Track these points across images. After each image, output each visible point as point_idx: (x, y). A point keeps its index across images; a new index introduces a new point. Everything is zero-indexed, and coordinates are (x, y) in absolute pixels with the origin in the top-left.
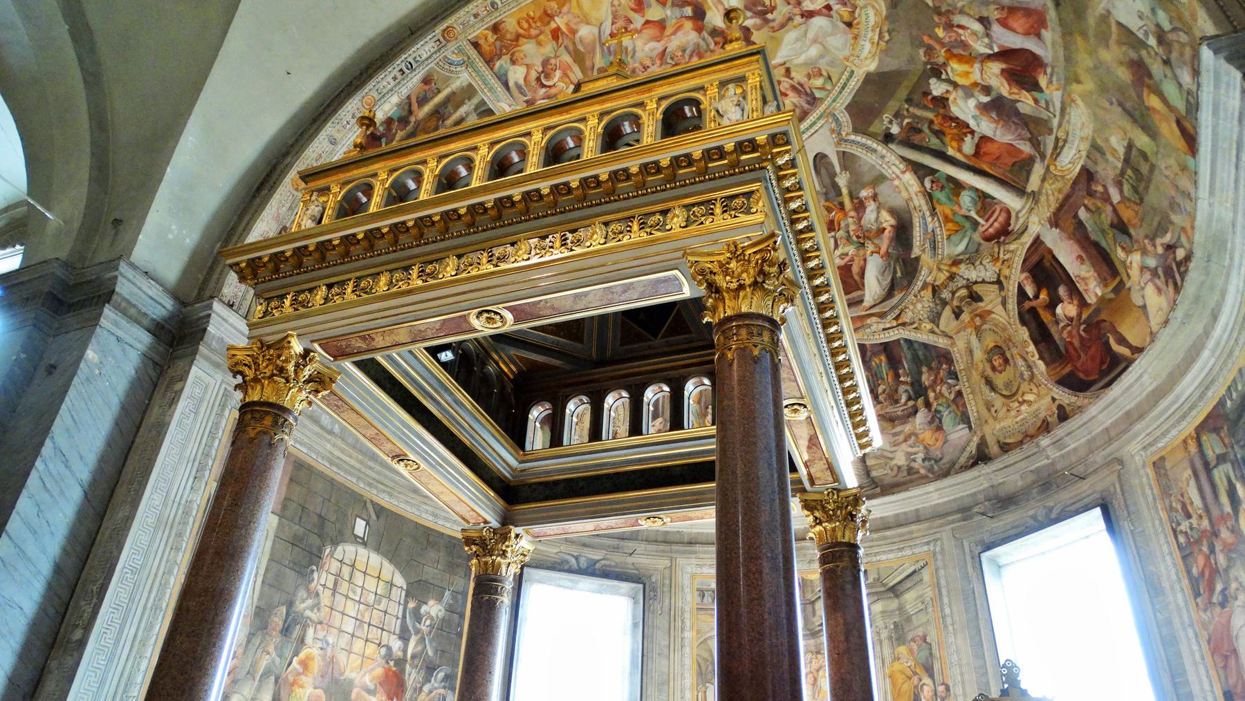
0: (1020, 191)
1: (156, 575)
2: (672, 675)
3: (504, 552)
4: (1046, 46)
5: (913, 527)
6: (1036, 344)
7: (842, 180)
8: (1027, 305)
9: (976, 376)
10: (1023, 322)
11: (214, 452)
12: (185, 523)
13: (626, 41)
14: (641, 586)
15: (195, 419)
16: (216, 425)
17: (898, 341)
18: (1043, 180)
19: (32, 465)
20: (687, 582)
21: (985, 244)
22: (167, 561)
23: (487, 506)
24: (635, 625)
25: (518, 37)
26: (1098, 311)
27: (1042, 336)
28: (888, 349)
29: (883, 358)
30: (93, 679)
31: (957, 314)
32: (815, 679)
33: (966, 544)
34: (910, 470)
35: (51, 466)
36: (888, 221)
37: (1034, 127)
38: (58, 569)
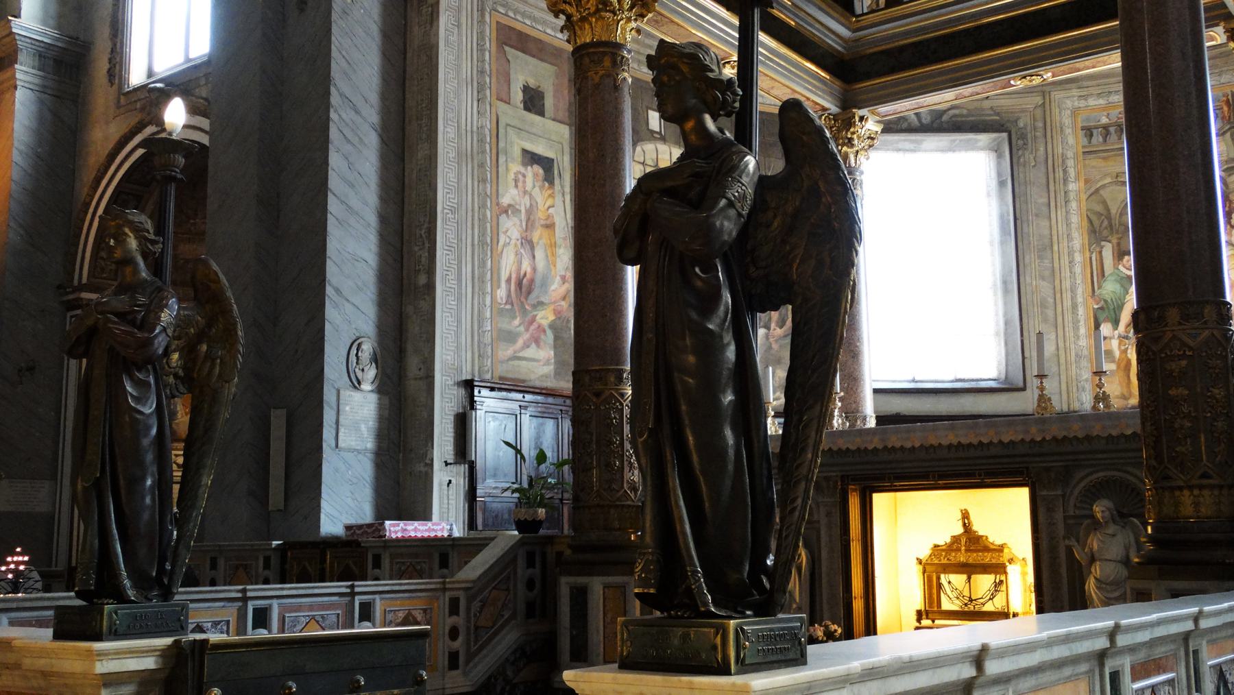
1: (473, 210)
2: (1055, 238)
3: (850, 140)
11: (487, 66)
12: (484, 152)
14: (1005, 135)
15: (459, 34)
16: (481, 36)
19: (328, 118)
20: (1067, 121)
22: (479, 196)
23: (823, 91)
24: (1002, 184)
30: (450, 319)
35: (344, 116)
38: (383, 219)
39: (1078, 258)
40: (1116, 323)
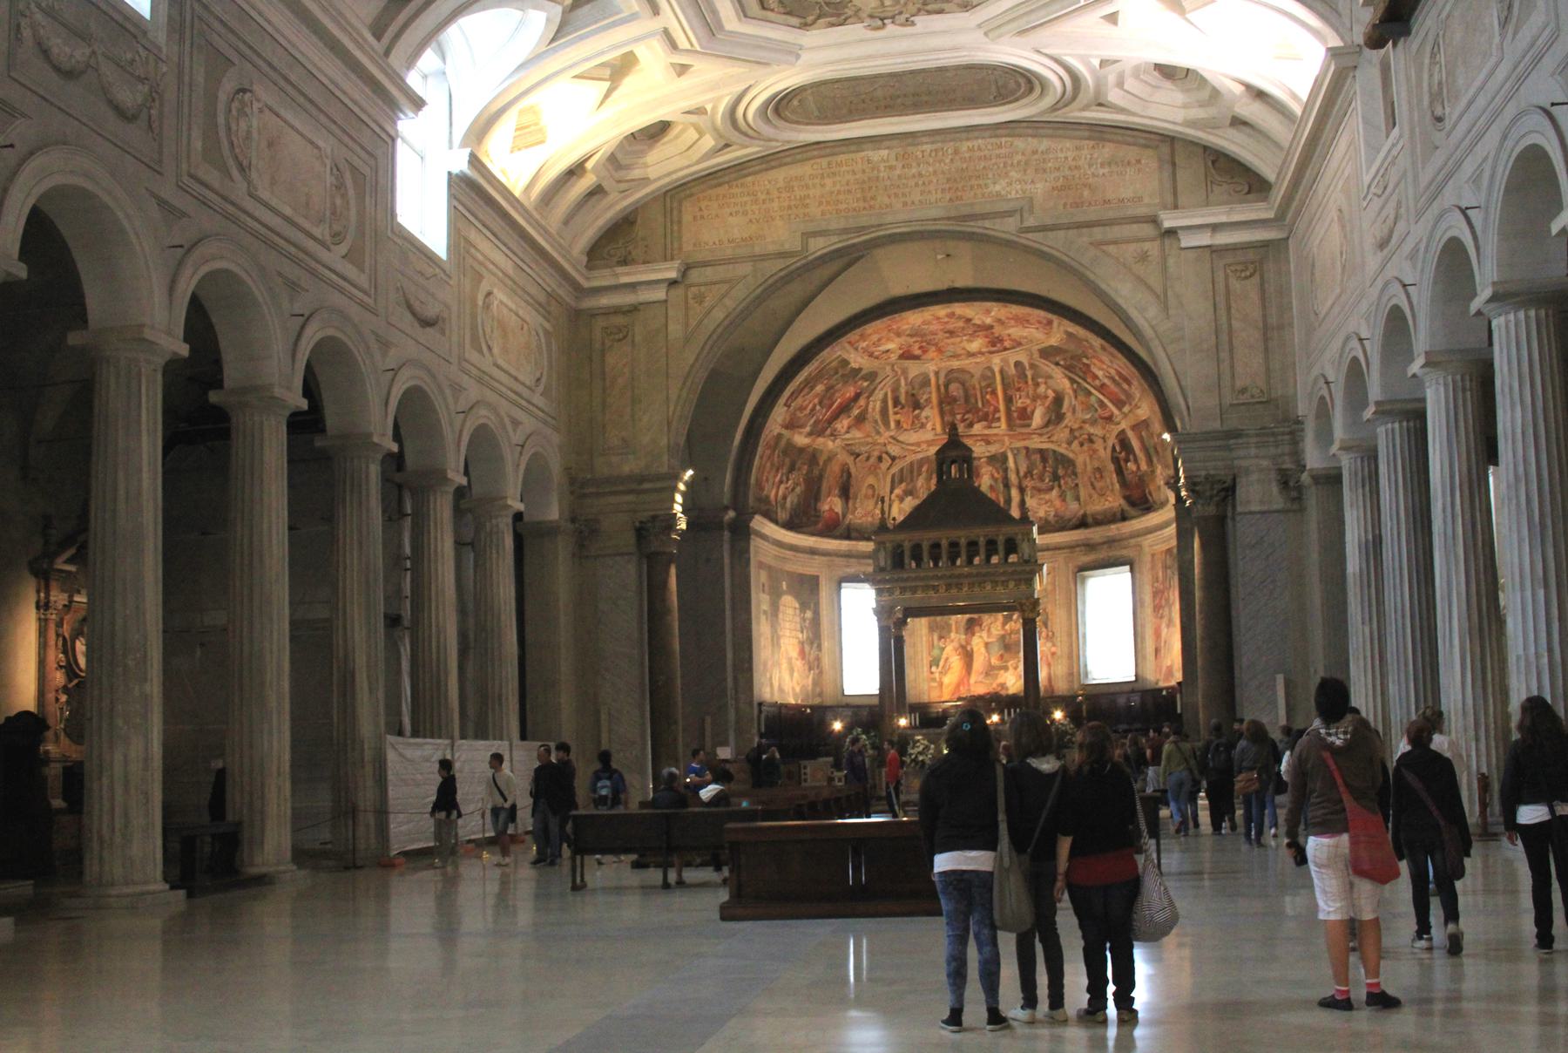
0: (1120, 409)
4: (1135, 383)
5: (1045, 553)
6: (1117, 474)
7: (1029, 373)
8: (1116, 455)
9: (1086, 479)
10: (1113, 462)
13: (926, 327)
17: (1047, 450)
18: (1130, 412)
21: (1100, 420)
25: (870, 335)
26: (1143, 475)
27: (1120, 471)
28: (1041, 451)
29: (1039, 456)
31: (1082, 445)
32: (989, 629)
33: (1070, 565)
34: (1046, 520)
36: (1051, 394)
37: (1129, 396)
39: (924, 639)
40: (938, 666)
